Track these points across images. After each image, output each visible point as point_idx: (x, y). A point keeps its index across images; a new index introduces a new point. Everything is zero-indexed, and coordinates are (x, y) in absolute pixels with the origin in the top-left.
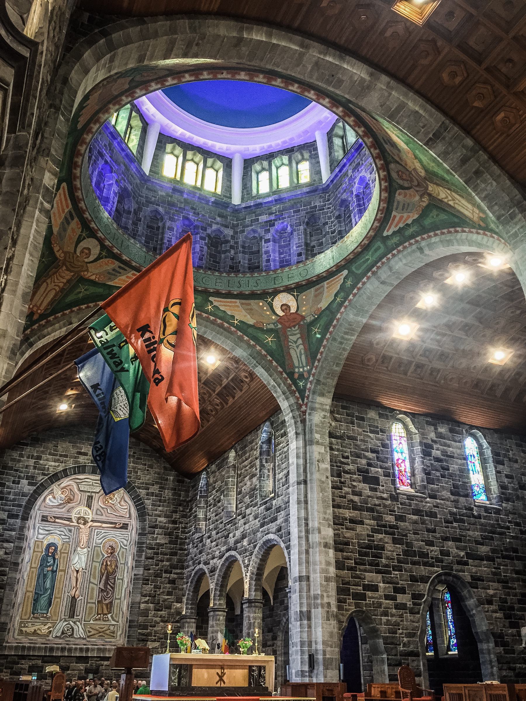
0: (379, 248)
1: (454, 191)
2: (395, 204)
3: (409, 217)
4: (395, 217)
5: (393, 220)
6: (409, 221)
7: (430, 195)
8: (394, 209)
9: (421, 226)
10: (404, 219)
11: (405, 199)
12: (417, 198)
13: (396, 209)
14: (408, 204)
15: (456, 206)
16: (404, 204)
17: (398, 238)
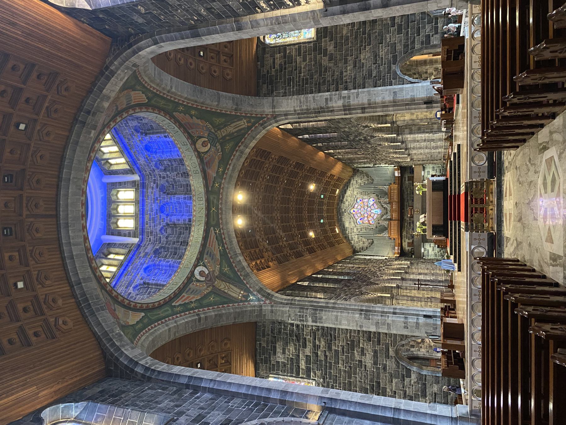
0: (168, 310)
1: (232, 284)
2: (187, 289)
3: (193, 298)
4: (184, 296)
5: (182, 298)
6: (193, 300)
7: (214, 286)
8: (185, 292)
9: (200, 303)
10: (190, 298)
11: (196, 287)
12: (206, 287)
13: (187, 292)
14: (197, 291)
15: (229, 292)
16: (194, 290)
17: (182, 308)
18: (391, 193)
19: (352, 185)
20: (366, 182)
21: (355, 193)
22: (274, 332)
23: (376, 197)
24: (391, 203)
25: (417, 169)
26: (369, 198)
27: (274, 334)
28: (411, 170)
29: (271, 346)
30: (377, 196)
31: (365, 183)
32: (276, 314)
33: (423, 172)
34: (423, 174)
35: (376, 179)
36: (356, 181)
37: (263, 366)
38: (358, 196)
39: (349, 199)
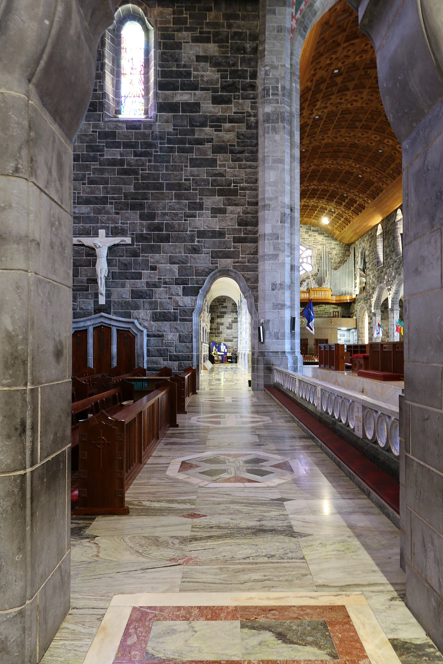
18: (321, 291)
19: (330, 243)
20: (333, 261)
21: (320, 247)
22: (236, 38)
23: (314, 273)
24: (308, 291)
25: (351, 322)
26: (313, 264)
27: (232, 38)
28: (349, 315)
29: (209, 33)
30: (316, 275)
31: (332, 259)
32: (275, 38)
33: (346, 329)
34: (342, 329)
35: (338, 273)
36: (335, 248)
37: (170, 15)
38: (316, 251)
39: (312, 239)
